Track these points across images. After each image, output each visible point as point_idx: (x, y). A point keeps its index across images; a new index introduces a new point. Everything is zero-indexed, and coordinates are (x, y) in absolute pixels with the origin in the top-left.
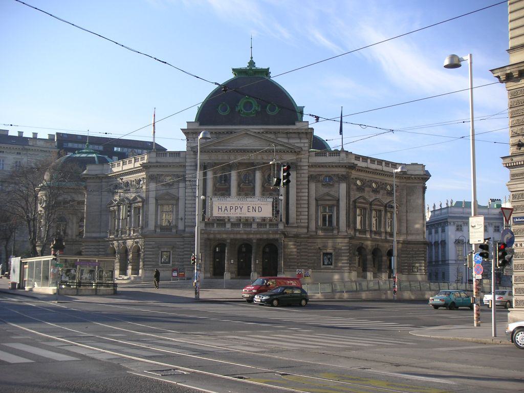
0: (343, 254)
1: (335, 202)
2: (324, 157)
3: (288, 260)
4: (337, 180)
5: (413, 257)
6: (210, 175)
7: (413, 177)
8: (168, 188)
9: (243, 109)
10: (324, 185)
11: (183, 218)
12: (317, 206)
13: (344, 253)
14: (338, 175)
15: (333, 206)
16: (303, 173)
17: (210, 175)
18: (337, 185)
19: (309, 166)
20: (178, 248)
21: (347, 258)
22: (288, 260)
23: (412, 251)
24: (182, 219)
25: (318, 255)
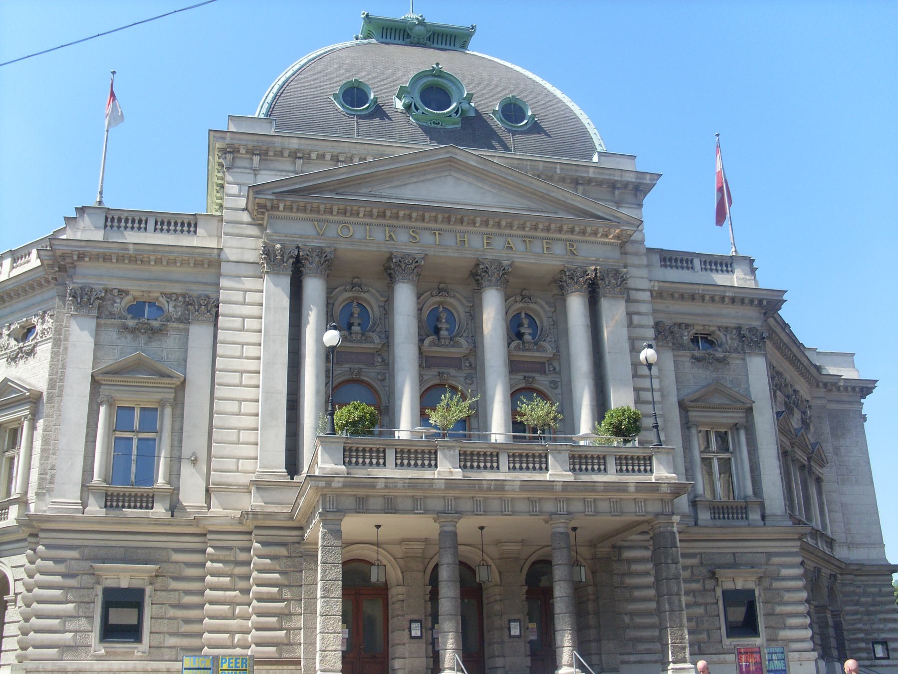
0: (787, 596)
1: (737, 417)
2: (685, 271)
3: (627, 619)
4: (735, 344)
5: (869, 613)
6: (314, 288)
7: (841, 383)
8: (143, 339)
9: (419, 103)
10: (698, 359)
11: (203, 456)
12: (687, 425)
13: (789, 590)
14: (739, 329)
15: (736, 427)
16: (638, 313)
17: (314, 288)
18: (735, 361)
19: (651, 292)
20: (176, 578)
21: (802, 608)
22: (627, 619)
23: (865, 594)
24: (195, 462)
25: (710, 600)
